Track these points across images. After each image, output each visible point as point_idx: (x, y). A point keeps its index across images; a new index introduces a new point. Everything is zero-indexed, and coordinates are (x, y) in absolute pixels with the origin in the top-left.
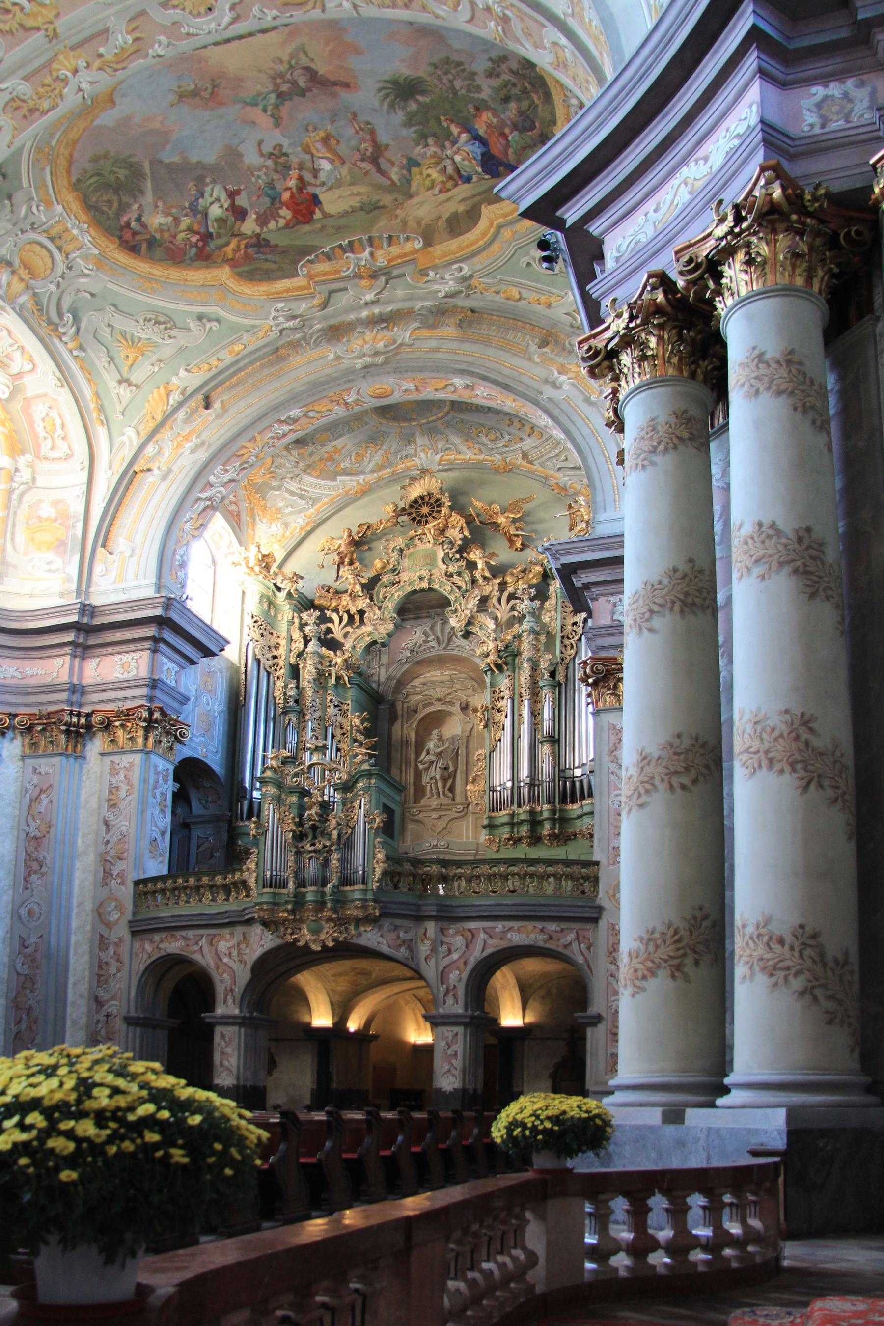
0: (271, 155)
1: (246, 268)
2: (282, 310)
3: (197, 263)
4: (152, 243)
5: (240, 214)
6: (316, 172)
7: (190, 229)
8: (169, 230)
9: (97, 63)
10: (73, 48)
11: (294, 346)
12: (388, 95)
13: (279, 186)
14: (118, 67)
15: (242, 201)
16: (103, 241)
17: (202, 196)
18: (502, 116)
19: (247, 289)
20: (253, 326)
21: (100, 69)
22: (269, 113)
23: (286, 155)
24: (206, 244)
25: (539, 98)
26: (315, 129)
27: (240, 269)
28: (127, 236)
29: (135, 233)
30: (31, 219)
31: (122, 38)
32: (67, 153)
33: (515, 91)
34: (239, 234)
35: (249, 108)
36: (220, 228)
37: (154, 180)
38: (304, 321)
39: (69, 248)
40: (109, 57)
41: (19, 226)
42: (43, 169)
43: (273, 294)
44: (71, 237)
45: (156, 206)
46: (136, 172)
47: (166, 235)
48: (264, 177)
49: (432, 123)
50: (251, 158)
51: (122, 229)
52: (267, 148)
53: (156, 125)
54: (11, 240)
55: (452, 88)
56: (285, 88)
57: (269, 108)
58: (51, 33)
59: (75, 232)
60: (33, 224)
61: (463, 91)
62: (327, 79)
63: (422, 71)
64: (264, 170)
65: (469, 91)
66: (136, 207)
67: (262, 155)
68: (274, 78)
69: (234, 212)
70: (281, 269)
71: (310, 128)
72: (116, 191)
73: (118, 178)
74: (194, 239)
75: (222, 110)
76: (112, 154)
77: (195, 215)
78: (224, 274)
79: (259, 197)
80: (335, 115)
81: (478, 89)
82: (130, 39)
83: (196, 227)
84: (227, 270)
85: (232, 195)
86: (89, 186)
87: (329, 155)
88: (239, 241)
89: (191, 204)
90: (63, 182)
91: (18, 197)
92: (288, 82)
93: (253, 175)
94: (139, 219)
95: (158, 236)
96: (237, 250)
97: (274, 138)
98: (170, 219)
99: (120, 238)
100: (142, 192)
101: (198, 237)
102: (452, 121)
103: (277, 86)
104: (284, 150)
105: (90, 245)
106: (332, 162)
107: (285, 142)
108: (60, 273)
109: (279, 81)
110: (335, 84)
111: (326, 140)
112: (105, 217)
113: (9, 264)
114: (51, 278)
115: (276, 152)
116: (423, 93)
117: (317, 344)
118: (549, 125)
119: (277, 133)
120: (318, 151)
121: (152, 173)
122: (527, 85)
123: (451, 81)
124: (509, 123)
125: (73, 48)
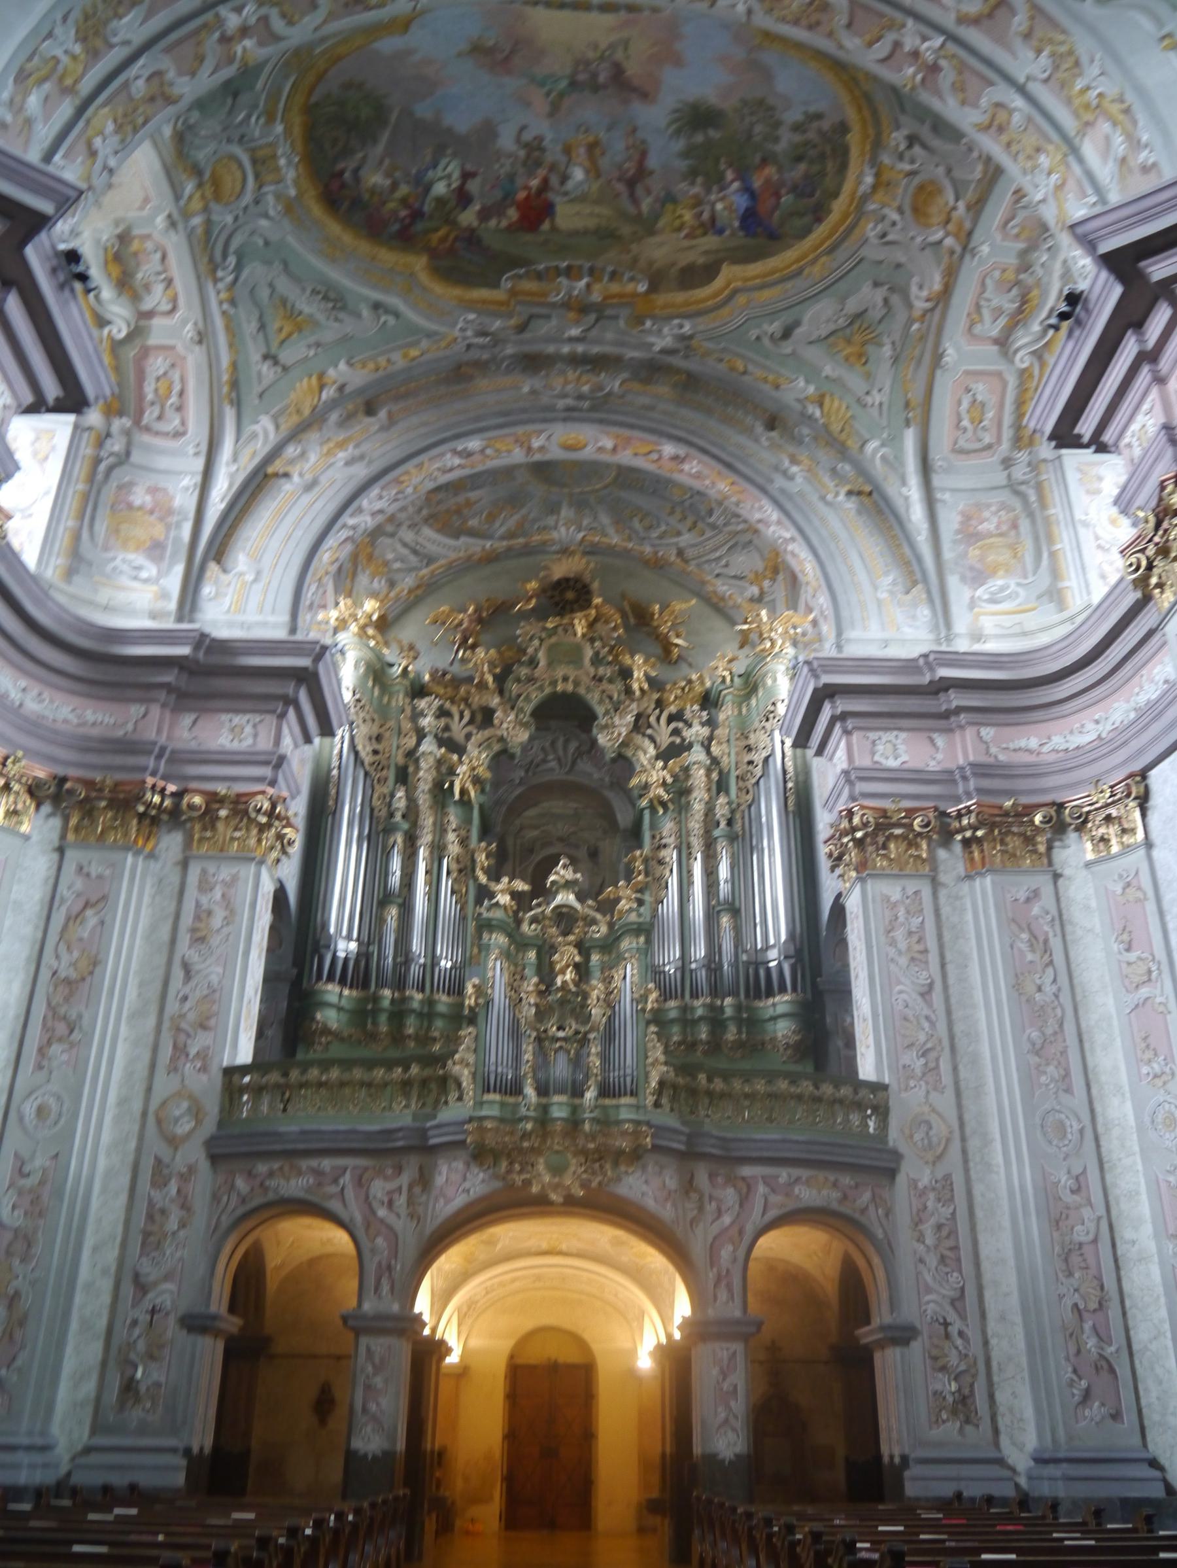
0: (527, 145)
2: (472, 321)
4: (357, 203)
6: (564, 178)
7: (404, 201)
11: (481, 366)
13: (520, 181)
15: (473, 186)
19: (439, 289)
20: (436, 333)
26: (586, 131)
29: (343, 186)
34: (453, 223)
38: (497, 340)
42: (286, 77)
46: (380, 114)
50: (506, 141)
52: (527, 136)
56: (582, 77)
57: (553, 95)
67: (518, 140)
78: (419, 263)
81: (776, 140)
85: (466, 176)
91: (244, 99)
94: (356, 171)
95: (366, 196)
96: (443, 240)
97: (540, 127)
98: (388, 182)
100: (375, 141)
106: (587, 172)
107: (549, 136)
117: (509, 371)
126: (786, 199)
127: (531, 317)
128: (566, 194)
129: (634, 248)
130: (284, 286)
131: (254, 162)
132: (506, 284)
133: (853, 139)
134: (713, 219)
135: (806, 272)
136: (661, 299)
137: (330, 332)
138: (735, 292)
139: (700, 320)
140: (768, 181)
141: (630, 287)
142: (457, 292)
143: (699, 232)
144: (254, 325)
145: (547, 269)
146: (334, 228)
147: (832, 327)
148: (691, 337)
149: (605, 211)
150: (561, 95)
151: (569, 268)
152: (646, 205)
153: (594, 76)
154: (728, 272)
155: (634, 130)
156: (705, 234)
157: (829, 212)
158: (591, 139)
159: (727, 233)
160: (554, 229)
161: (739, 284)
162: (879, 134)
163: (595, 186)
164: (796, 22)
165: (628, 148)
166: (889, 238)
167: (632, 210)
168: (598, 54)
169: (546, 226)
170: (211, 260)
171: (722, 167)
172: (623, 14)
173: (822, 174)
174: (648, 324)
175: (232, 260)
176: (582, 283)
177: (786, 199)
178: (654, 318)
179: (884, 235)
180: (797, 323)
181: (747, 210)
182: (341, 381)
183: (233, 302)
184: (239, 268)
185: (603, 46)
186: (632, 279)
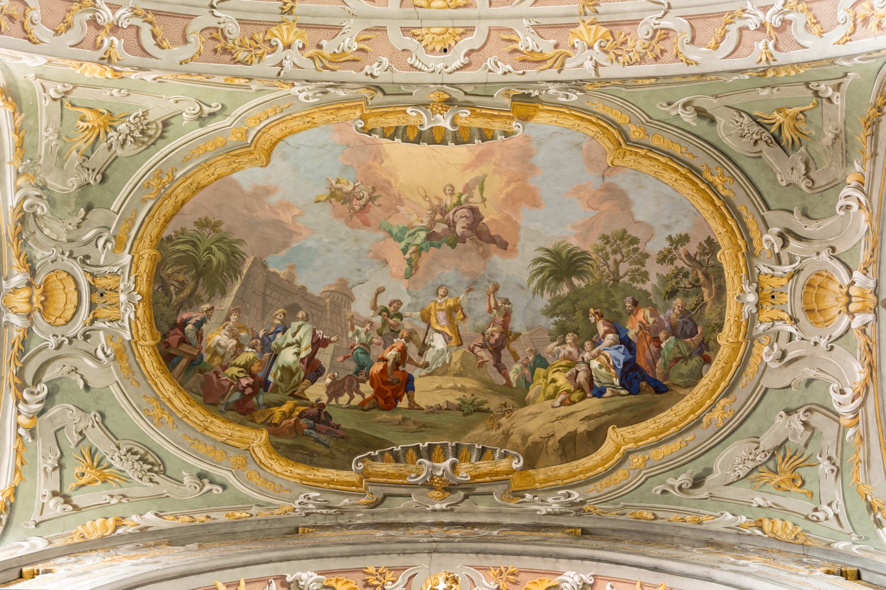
1: (289, 442)
2: (315, 499)
3: (231, 414)
4: (195, 363)
5: (313, 370)
6: (424, 347)
7: (247, 368)
8: (223, 357)
9: (312, 51)
10: (300, 26)
12: (541, 270)
13: (375, 352)
14: (328, 65)
15: (324, 357)
16: (144, 330)
17: (284, 331)
18: (662, 316)
19: (278, 465)
20: (269, 504)
21: (311, 58)
22: (408, 256)
23: (400, 316)
24: (255, 393)
25: (710, 295)
26: (446, 294)
27: (279, 440)
28: (173, 339)
29: (183, 340)
30: (89, 250)
31: (348, 42)
32: (181, 197)
33: (685, 283)
34: (300, 398)
35: (391, 241)
36: (282, 380)
37: (243, 285)
39: (102, 312)
40: (326, 52)
41: (72, 246)
42: (145, 201)
43: (310, 480)
44: (114, 300)
45: (228, 319)
46: (234, 258)
47: (217, 361)
48: (363, 335)
49: (579, 314)
50: (362, 307)
51: (175, 325)
52: (384, 301)
53: (286, 217)
54: (55, 253)
55: (616, 272)
56: (439, 228)
57: (411, 250)
58: (287, 8)
59: (123, 297)
60: (88, 257)
61: (626, 279)
62: (488, 231)
63: (588, 245)
64: (368, 326)
65: (633, 279)
66: (207, 306)
67: (374, 308)
68: (435, 212)
69: (307, 366)
70: (332, 457)
71: (441, 292)
72: (199, 275)
73: (210, 261)
74: (244, 382)
75: (363, 232)
76: (223, 228)
77: (263, 352)
78: (258, 438)
79: (345, 358)
80: (475, 283)
81: (645, 276)
82: (355, 46)
83: (255, 368)
84: (264, 435)
85: (318, 343)
86: (174, 252)
87: (447, 330)
88: (296, 405)
89: (266, 335)
90: (153, 230)
91: (97, 215)
92: (447, 222)
93: (353, 329)
94: (199, 325)
95: (206, 357)
96: (286, 416)
99: (165, 336)
100: (224, 293)
101: (251, 380)
102: (602, 316)
103: (433, 222)
104: (400, 310)
105: (126, 324)
106: (448, 338)
107: (406, 300)
108: (71, 334)
109: (438, 217)
110: (492, 240)
111: (451, 311)
112: (167, 299)
113: (33, 272)
114: (57, 331)
115: (391, 309)
116: (580, 274)
118: (714, 331)
119: (403, 285)
120: (438, 322)
121: (248, 275)
122: (701, 276)
123: (617, 263)
124: (667, 324)
125: (300, 26)
126: (668, 343)
127: (385, 496)
128: (426, 365)
129: (503, 420)
130: (95, 436)
131: (92, 289)
132: (358, 466)
133: (725, 257)
134: (590, 379)
135: (705, 420)
136: (540, 474)
137: (142, 488)
138: (628, 454)
139: (591, 487)
140: (643, 327)
141: (503, 464)
142: (300, 470)
143: (575, 396)
144: (52, 462)
145: (405, 450)
146: (167, 388)
147: (751, 465)
148: (583, 503)
149: (469, 383)
150: (419, 250)
151: (431, 448)
152: (514, 372)
153: (452, 225)
154: (614, 435)
155: (496, 288)
156: (584, 398)
157: (719, 346)
158: (451, 303)
159: (608, 393)
160: (413, 406)
161: (631, 446)
162: (749, 241)
163: (457, 356)
164: (642, 60)
165: (490, 311)
166: (790, 356)
167: (500, 380)
168: (455, 200)
169: (404, 403)
170: (20, 374)
171: (592, 319)
172: (478, 145)
173: (700, 305)
174: (528, 496)
175: (43, 390)
176: (447, 464)
177: (668, 343)
178: (534, 491)
179: (784, 354)
180: (709, 471)
181: (625, 363)
182: (143, 524)
183: (32, 432)
184: (49, 399)
185: (459, 189)
186: (505, 456)
